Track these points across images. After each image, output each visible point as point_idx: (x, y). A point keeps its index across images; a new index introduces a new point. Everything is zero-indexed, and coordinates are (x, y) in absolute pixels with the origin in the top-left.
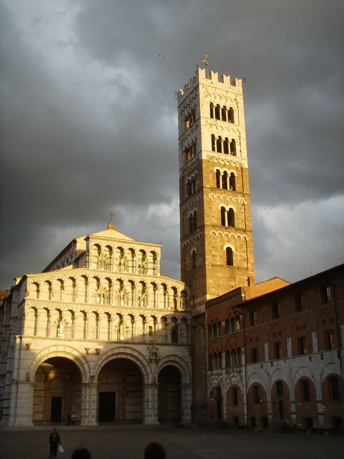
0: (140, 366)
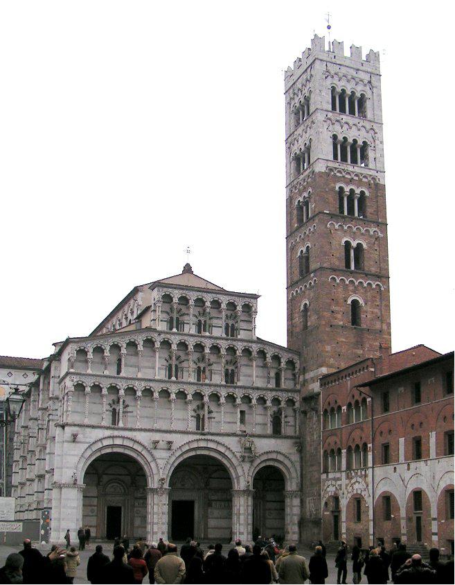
0: (228, 465)
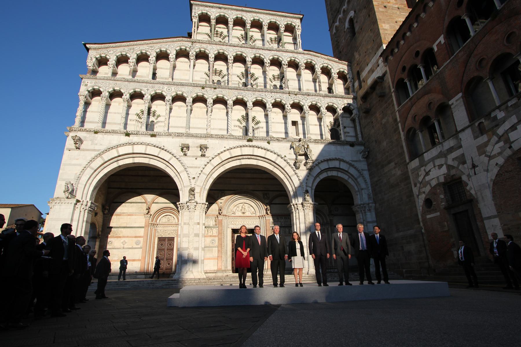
0: (282, 176)
